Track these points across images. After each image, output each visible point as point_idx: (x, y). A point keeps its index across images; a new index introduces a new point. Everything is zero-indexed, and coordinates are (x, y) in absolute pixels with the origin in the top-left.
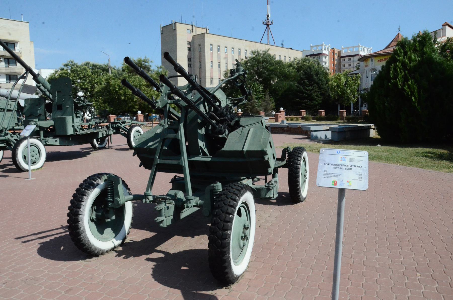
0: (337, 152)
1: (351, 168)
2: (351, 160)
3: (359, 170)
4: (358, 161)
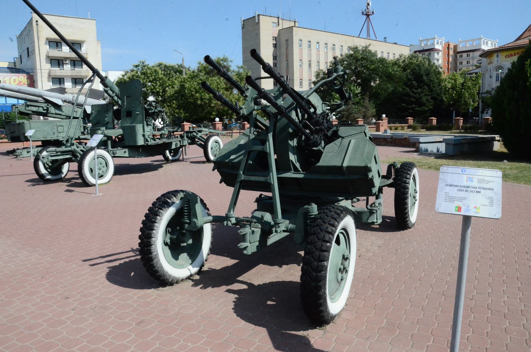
0: (462, 171)
1: (479, 190)
2: (479, 181)
3: (489, 193)
4: (488, 182)
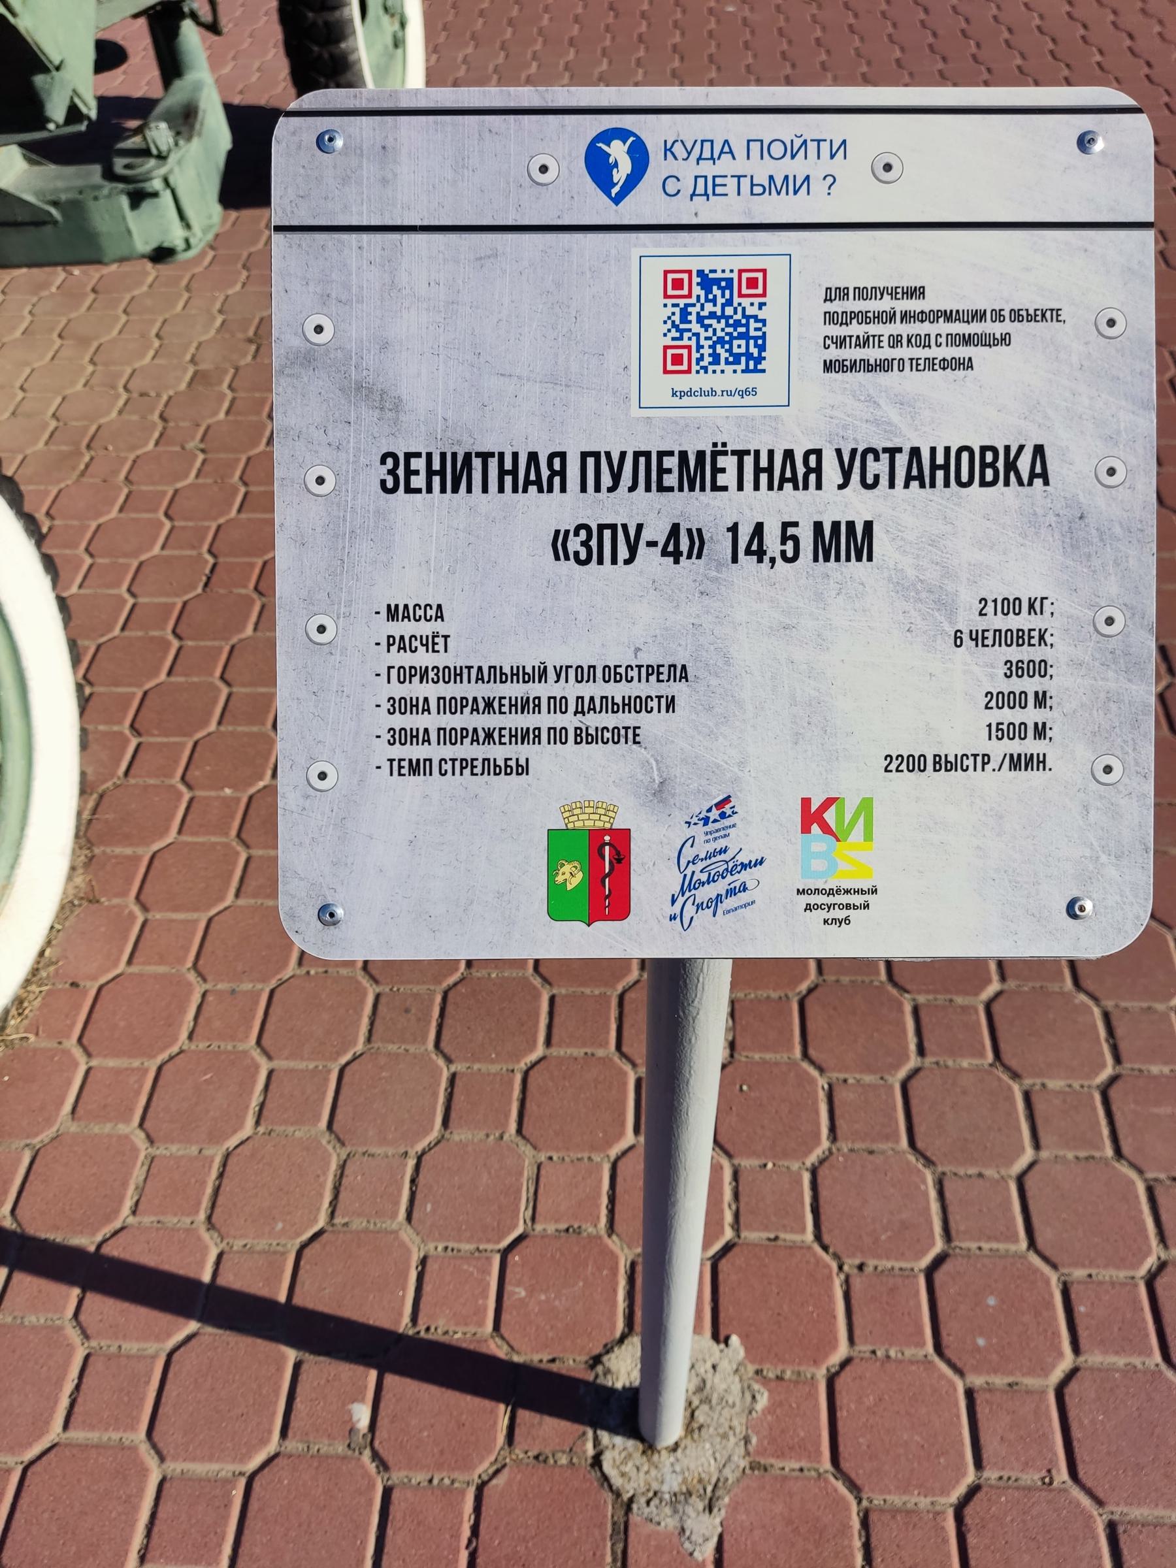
1: (854, 505)
4: (977, 330)
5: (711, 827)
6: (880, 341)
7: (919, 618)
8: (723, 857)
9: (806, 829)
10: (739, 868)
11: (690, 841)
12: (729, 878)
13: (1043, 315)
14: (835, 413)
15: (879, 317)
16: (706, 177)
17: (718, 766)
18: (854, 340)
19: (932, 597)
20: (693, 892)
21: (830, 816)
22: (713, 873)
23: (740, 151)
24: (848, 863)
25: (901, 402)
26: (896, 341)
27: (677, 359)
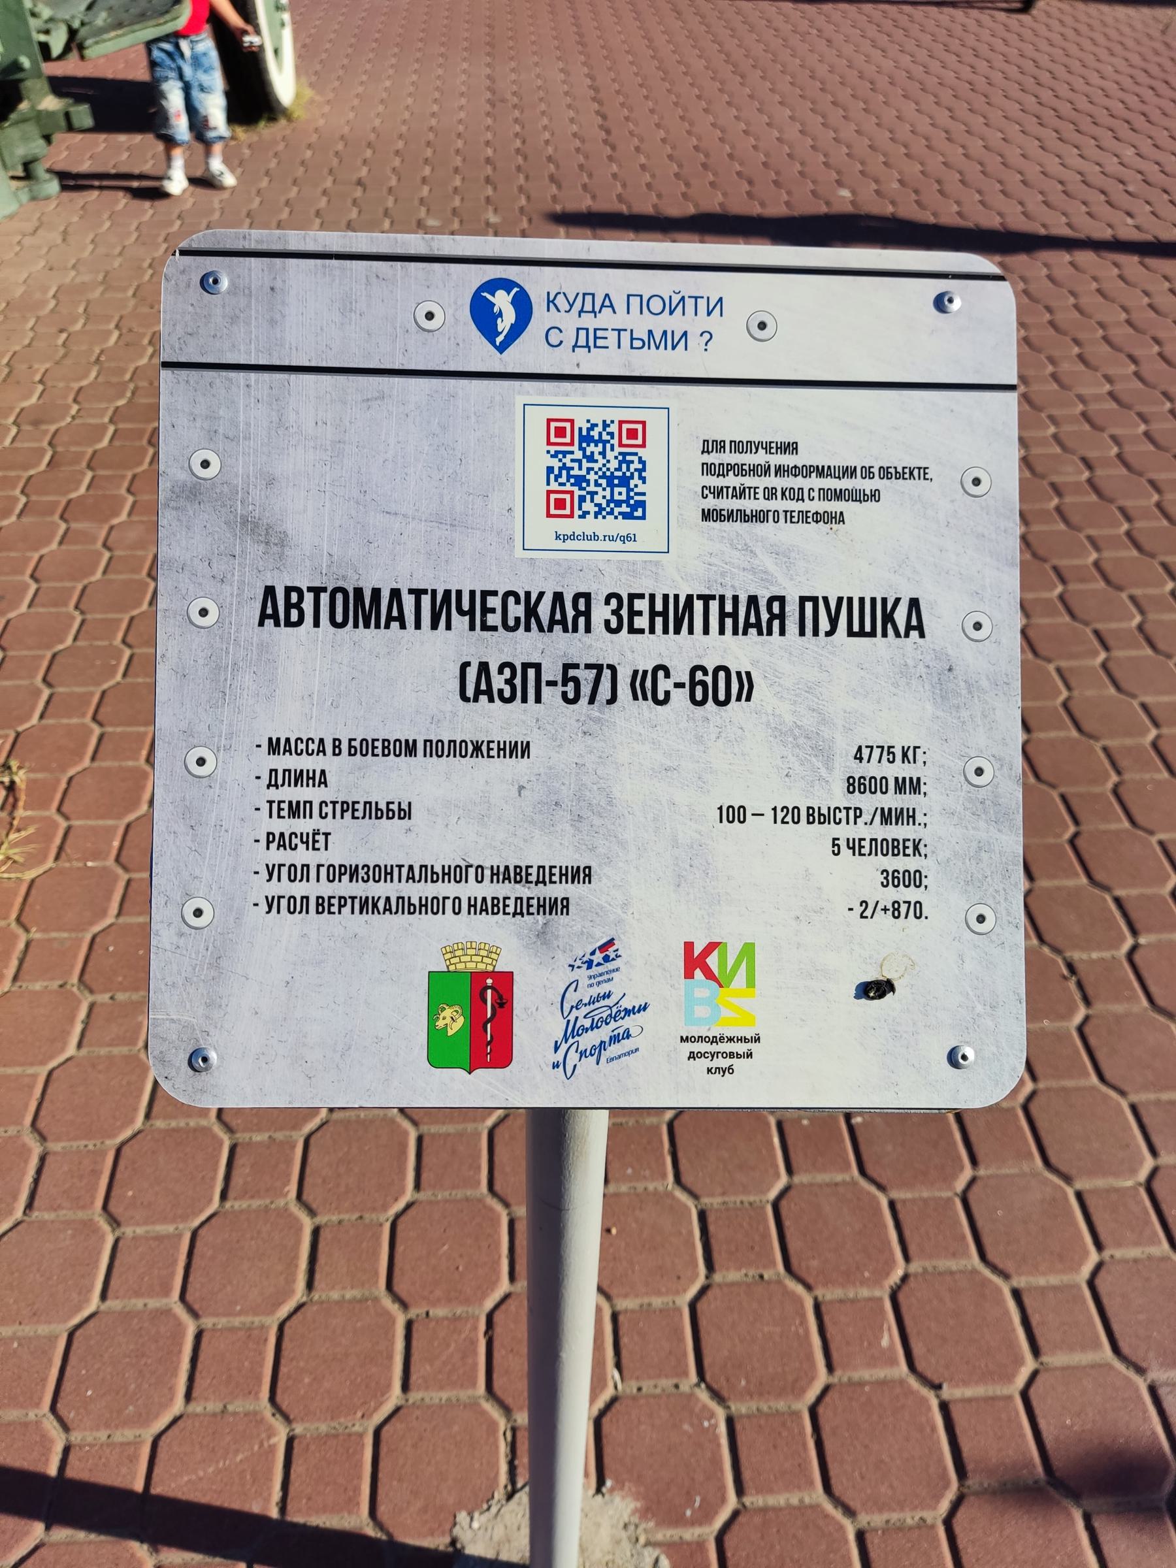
0: (483, 314)
4: (846, 487)
5: (595, 970)
6: (755, 493)
7: (797, 764)
8: (607, 1002)
9: (689, 975)
10: (623, 1014)
11: (574, 985)
12: (613, 1025)
13: (911, 473)
14: (713, 560)
15: (754, 470)
16: (587, 330)
17: (602, 908)
18: (730, 490)
19: (809, 743)
20: (577, 1038)
21: (712, 961)
22: (596, 1018)
23: (620, 305)
24: (728, 1010)
25: (776, 552)
26: (770, 494)
27: (560, 504)
